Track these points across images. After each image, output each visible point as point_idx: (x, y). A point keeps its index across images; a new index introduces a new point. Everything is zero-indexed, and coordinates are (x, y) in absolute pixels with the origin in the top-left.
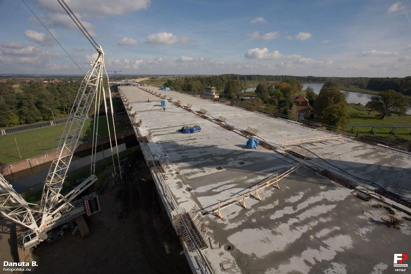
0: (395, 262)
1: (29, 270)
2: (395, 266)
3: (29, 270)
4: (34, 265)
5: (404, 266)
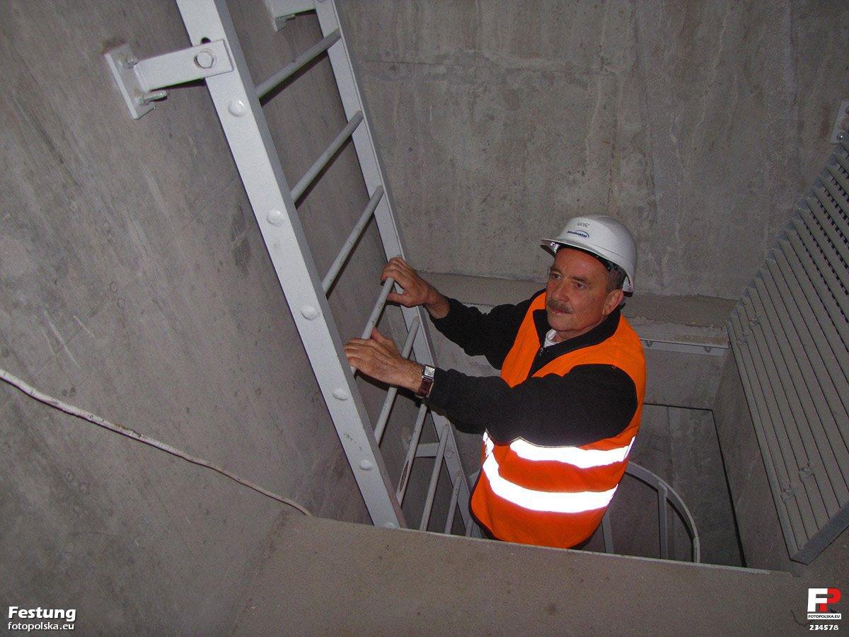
0: (811, 607)
1: (71, 627)
2: (810, 618)
3: (71, 627)
4: (71, 614)
5: (832, 618)
